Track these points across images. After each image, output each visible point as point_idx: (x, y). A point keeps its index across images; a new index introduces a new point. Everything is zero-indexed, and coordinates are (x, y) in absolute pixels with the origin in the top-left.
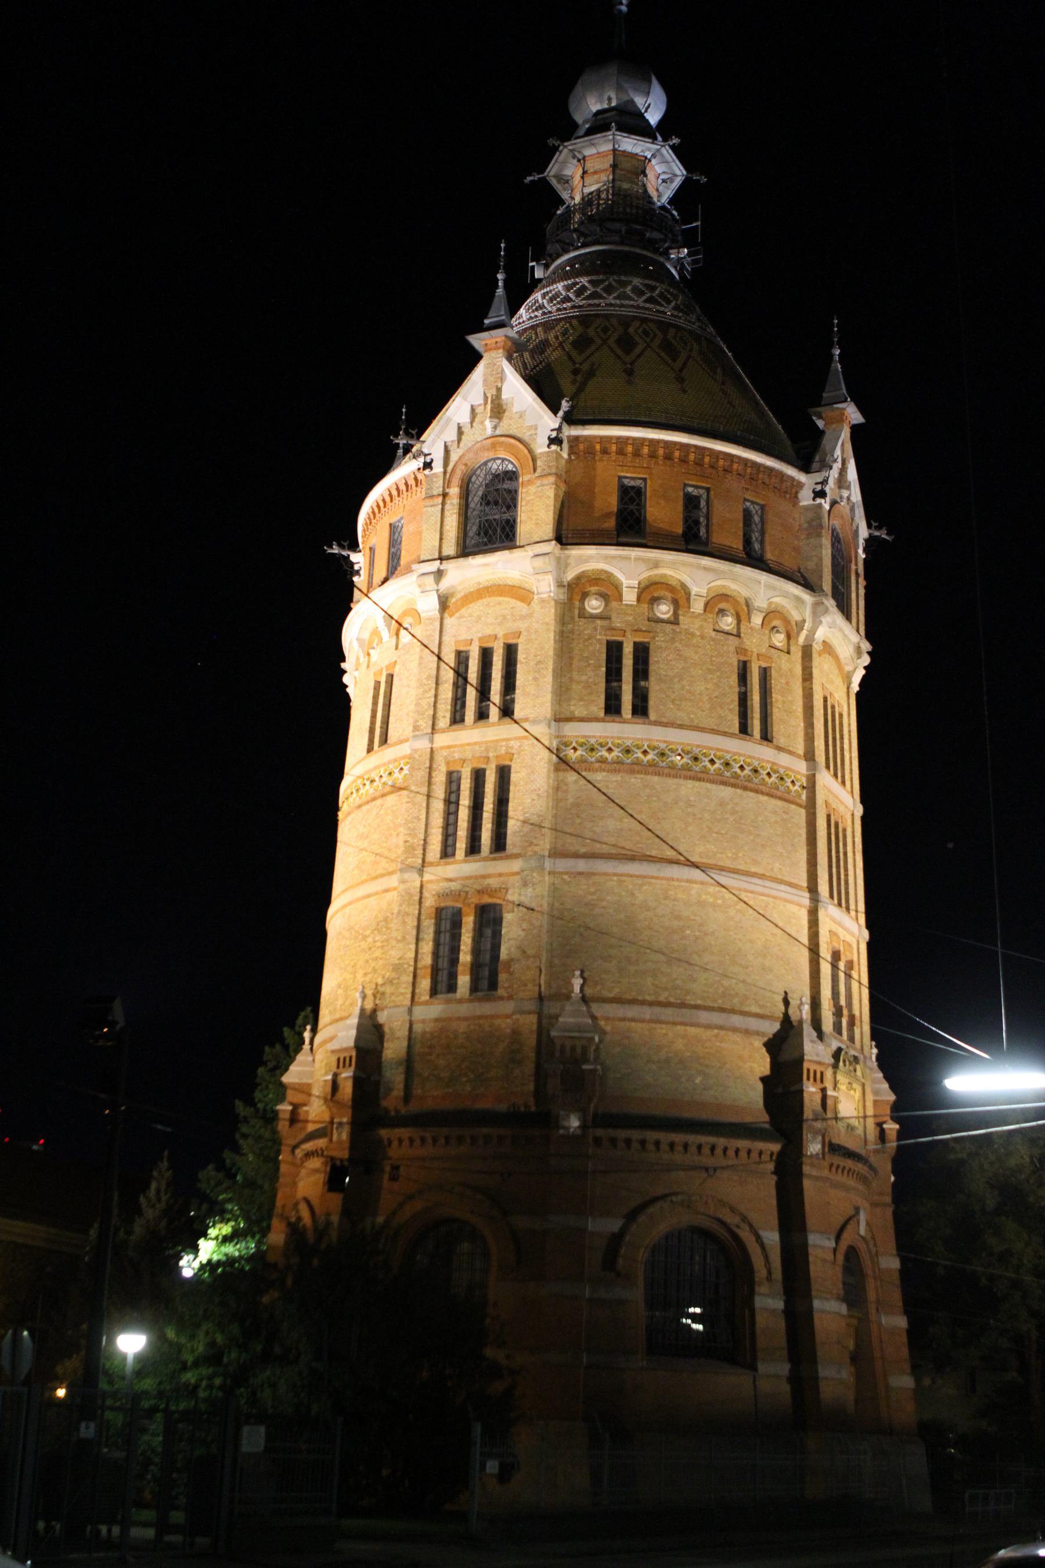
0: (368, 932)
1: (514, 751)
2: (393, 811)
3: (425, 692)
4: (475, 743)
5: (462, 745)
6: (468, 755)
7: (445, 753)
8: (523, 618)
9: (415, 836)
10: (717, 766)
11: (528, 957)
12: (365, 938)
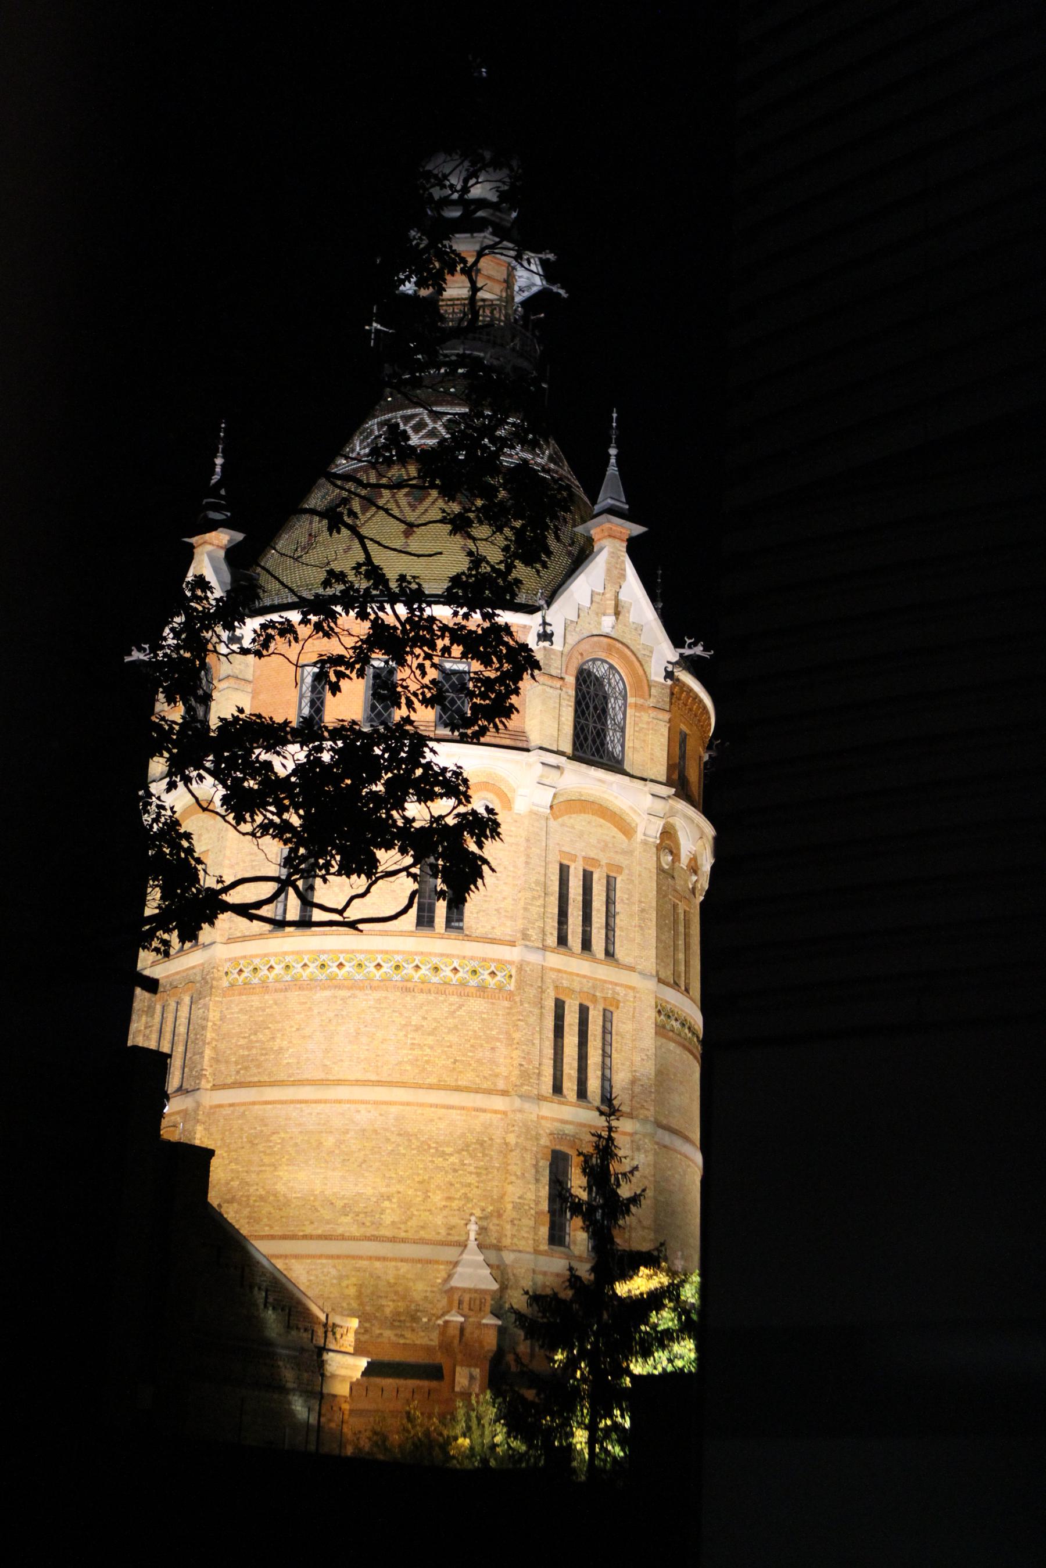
0: (449, 1150)
1: (620, 998)
2: (483, 1020)
3: (534, 898)
4: (584, 977)
5: (571, 974)
6: (577, 987)
7: (553, 975)
8: (624, 853)
9: (530, 1062)
10: (460, 974)
11: (644, 1228)
12: (443, 1154)
